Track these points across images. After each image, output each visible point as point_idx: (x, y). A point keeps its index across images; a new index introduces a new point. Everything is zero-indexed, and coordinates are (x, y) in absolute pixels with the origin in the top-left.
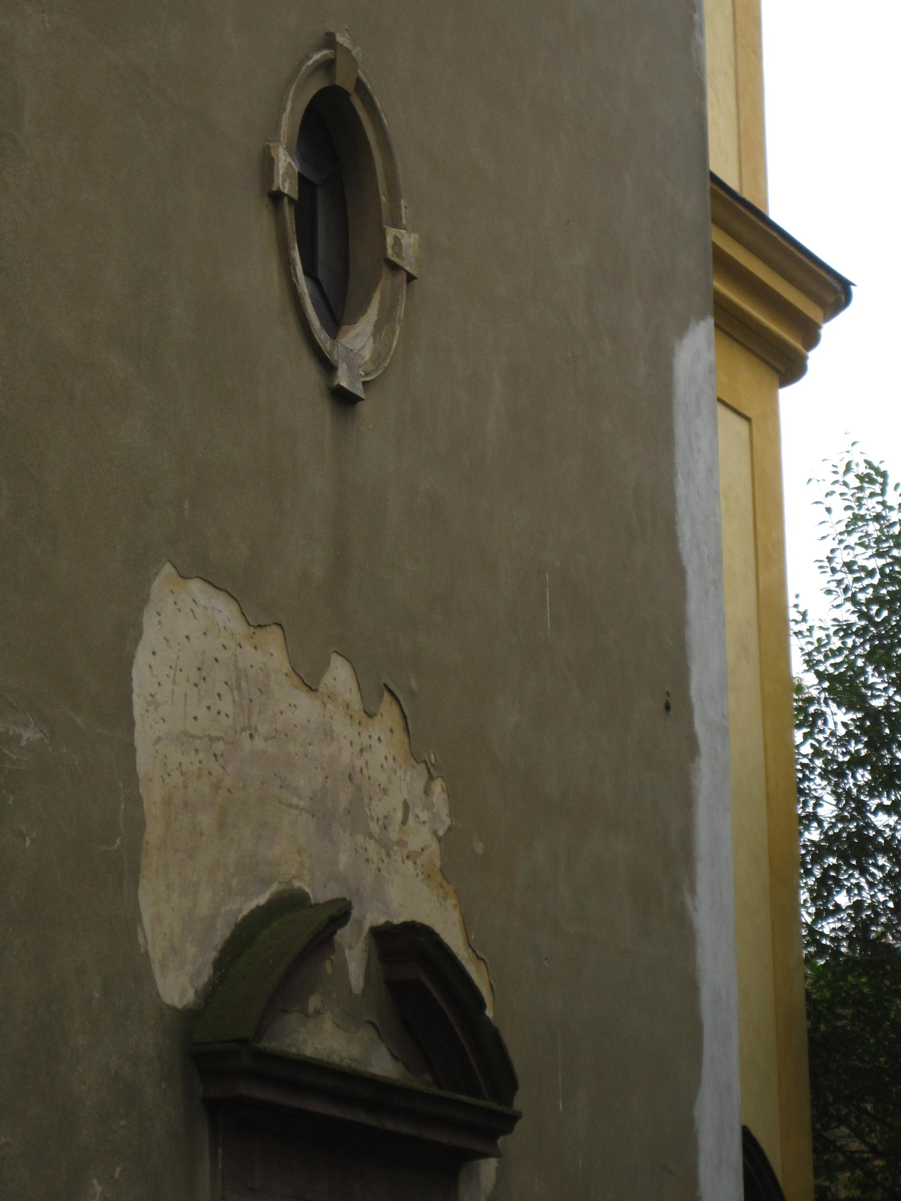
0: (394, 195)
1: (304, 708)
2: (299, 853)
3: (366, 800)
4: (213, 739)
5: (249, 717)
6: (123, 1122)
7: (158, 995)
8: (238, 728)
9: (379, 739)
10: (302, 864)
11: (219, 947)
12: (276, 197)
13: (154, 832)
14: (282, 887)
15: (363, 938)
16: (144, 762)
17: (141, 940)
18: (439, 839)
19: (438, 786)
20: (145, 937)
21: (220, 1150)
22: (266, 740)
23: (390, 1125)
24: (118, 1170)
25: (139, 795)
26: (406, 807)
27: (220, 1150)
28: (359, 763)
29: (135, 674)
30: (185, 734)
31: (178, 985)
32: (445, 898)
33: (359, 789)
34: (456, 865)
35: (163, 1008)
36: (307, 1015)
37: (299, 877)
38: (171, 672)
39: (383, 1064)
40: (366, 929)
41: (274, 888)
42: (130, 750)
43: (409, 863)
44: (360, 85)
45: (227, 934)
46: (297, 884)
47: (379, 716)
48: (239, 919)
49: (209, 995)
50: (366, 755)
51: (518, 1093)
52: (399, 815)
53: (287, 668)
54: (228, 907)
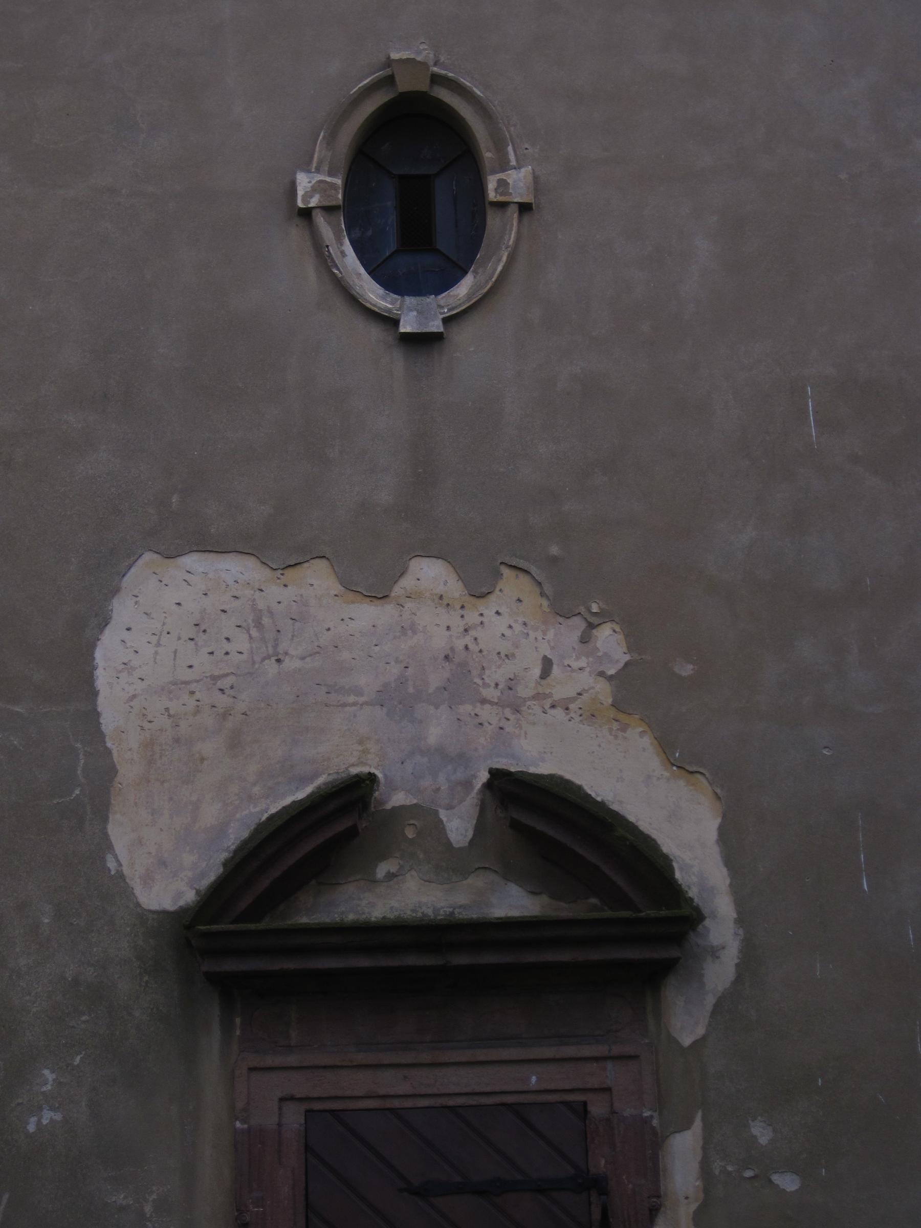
0: (499, 146)
2: (361, 742)
3: (475, 673)
4: (215, 678)
5: (276, 646)
6: (84, 1018)
7: (138, 905)
8: (257, 659)
9: (498, 613)
10: (365, 751)
11: (233, 847)
12: (306, 214)
14: (331, 778)
15: (474, 793)
17: (111, 864)
18: (610, 678)
20: (118, 861)
21: (238, 1021)
22: (303, 658)
23: (462, 960)
24: (78, 1059)
25: (106, 748)
26: (547, 666)
27: (238, 1021)
28: (460, 644)
29: (98, 654)
30: (175, 684)
32: (624, 728)
35: (142, 915)
36: (375, 881)
38: (154, 639)
39: (513, 902)
41: (321, 780)
42: (92, 716)
43: (559, 713)
44: (436, 79)
45: (245, 834)
47: (497, 592)
48: (264, 818)
50: (473, 633)
52: (537, 671)
53: (337, 588)
54: (247, 812)
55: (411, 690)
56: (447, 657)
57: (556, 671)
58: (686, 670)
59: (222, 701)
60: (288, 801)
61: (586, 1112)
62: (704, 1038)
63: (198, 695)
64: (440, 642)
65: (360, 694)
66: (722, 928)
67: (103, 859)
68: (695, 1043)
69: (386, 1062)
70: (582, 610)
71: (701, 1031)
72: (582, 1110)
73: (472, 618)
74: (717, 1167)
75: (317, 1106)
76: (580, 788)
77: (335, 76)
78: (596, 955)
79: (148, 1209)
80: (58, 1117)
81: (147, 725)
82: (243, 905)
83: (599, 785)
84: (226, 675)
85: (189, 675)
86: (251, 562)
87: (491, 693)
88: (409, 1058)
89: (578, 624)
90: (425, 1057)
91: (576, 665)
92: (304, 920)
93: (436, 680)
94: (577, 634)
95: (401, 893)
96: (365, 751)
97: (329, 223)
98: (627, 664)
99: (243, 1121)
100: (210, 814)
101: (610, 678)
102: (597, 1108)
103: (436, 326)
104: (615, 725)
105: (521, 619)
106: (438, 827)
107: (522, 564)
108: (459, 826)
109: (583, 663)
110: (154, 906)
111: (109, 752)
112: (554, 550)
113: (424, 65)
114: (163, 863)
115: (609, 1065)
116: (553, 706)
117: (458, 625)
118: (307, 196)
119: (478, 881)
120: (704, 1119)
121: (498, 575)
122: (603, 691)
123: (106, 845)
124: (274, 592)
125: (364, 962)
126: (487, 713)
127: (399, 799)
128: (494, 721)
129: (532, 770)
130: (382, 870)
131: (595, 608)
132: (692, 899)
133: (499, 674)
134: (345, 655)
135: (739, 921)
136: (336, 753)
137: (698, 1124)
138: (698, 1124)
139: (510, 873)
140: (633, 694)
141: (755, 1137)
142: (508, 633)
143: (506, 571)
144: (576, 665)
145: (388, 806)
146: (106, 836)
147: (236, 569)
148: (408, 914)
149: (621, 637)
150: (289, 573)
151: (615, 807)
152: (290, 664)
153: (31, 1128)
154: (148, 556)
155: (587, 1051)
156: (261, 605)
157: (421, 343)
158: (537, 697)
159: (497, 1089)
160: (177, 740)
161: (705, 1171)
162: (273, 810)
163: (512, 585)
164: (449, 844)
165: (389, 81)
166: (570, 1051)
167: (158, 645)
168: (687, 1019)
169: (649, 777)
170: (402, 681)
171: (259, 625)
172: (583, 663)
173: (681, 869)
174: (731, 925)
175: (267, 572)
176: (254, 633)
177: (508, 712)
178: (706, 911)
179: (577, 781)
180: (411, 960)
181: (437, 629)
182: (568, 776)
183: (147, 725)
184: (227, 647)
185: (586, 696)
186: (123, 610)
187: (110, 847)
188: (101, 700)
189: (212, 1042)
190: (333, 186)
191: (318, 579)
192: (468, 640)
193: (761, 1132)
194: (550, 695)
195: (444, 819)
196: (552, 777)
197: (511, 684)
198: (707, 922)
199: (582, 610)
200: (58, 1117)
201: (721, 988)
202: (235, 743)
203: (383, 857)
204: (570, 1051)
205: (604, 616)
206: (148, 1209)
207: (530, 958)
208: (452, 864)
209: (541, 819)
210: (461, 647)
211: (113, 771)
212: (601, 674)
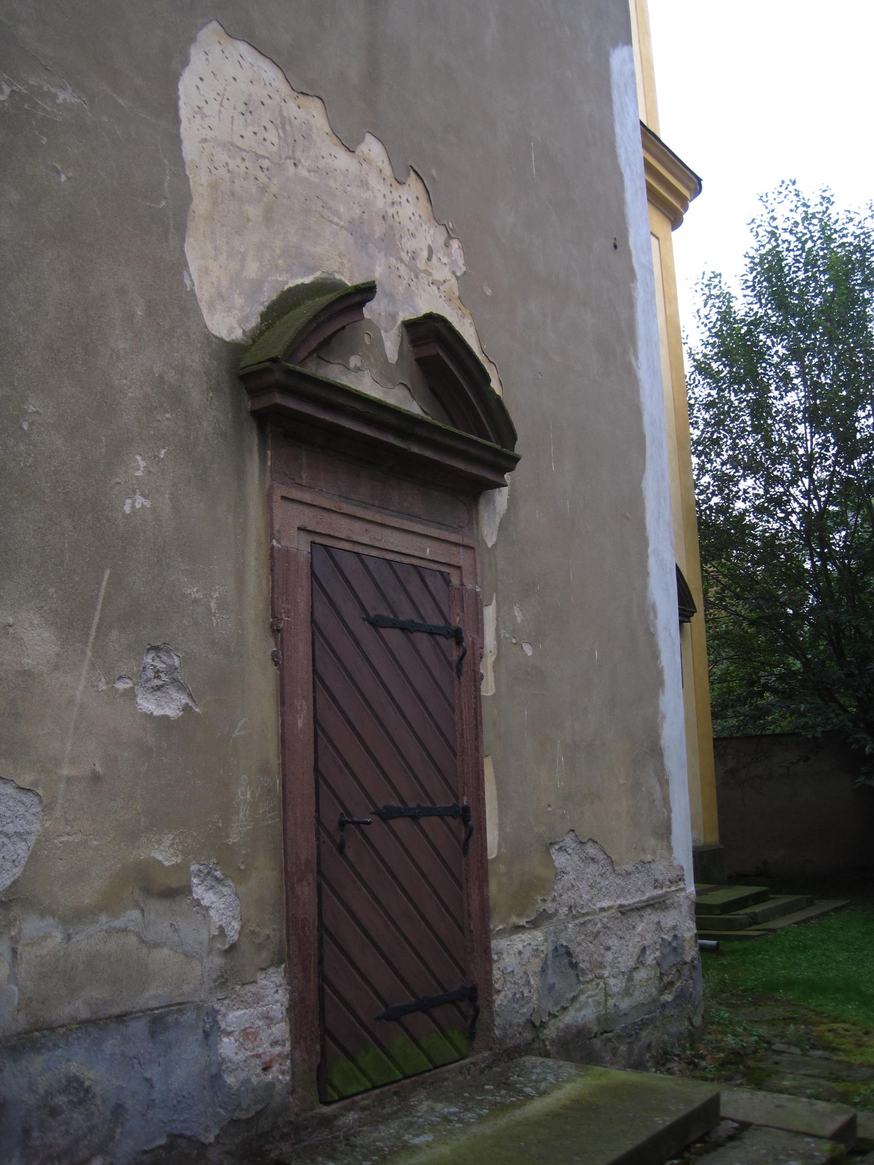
1: (343, 160)
2: (340, 255)
3: (397, 237)
4: (258, 156)
5: (294, 151)
6: (168, 415)
7: (205, 326)
8: (283, 156)
9: (407, 200)
10: (342, 264)
11: (266, 304)
13: (200, 205)
14: (324, 276)
15: (396, 327)
16: (190, 149)
17: (187, 281)
18: (457, 278)
19: (455, 244)
20: (192, 280)
21: (269, 452)
22: (309, 171)
23: (415, 449)
24: (163, 452)
25: (185, 175)
27: (269, 452)
29: (181, 86)
33: (391, 227)
34: (468, 291)
35: (209, 337)
40: (399, 322)
41: (318, 274)
42: (177, 140)
43: (434, 288)
45: (274, 297)
46: (338, 277)
48: (285, 289)
49: (256, 336)
51: (517, 443)
52: (425, 254)
53: (327, 129)
54: (274, 278)
60: (299, 281)
64: (380, 203)
65: (340, 219)
69: (358, 515)
71: (495, 539)
74: (502, 632)
75: (318, 540)
79: (213, 605)
80: (148, 504)
81: (214, 171)
84: (265, 157)
85: (239, 143)
90: (378, 518)
99: (278, 542)
100: (252, 269)
110: (216, 333)
114: (221, 296)
115: (461, 550)
120: (497, 600)
137: (494, 602)
138: (494, 602)
143: (412, 174)
153: (127, 509)
159: (411, 553)
161: (498, 637)
162: (292, 284)
175: (285, 88)
180: (391, 439)
183: (214, 171)
187: (186, 265)
189: (253, 466)
200: (148, 504)
202: (268, 216)
203: (353, 353)
206: (213, 605)
208: (386, 375)
211: (187, 197)
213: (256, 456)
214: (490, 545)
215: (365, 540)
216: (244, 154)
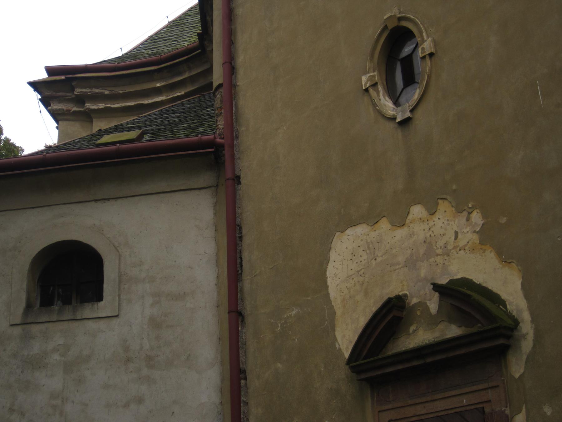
1: (400, 233)
2: (401, 282)
3: (434, 245)
4: (358, 271)
9: (439, 219)
10: (403, 285)
13: (339, 312)
17: (337, 346)
18: (478, 232)
22: (382, 256)
23: (429, 360)
26: (456, 233)
28: (428, 235)
29: (328, 273)
31: (347, 355)
37: (403, 290)
39: (454, 331)
43: (462, 251)
44: (400, 19)
47: (438, 210)
50: (432, 229)
52: (453, 238)
53: (389, 226)
55: (415, 258)
56: (424, 242)
57: (460, 236)
58: (503, 220)
59: (361, 279)
61: (484, 411)
62: (523, 374)
63: (354, 279)
64: (422, 237)
66: (527, 327)
67: (335, 345)
68: (521, 376)
69: (417, 402)
70: (466, 208)
72: (483, 410)
73: (431, 223)
76: (471, 280)
77: (371, 32)
78: (473, 349)
81: (342, 294)
82: (364, 353)
83: (478, 278)
85: (351, 273)
86: (365, 226)
87: (439, 251)
88: (424, 399)
89: (465, 213)
90: (429, 399)
91: (465, 231)
92: (390, 353)
93: (422, 251)
94: (465, 218)
95: (419, 336)
96: (403, 285)
97: (374, 90)
98: (483, 225)
101: (478, 232)
102: (487, 410)
103: (408, 114)
104: (481, 251)
105: (446, 219)
106: (427, 308)
107: (444, 196)
108: (433, 306)
109: (468, 229)
111: (333, 306)
112: (454, 187)
113: (395, 16)
115: (489, 391)
116: (460, 250)
117: (427, 227)
118: (366, 83)
119: (441, 326)
120: (526, 408)
121: (437, 204)
122: (476, 238)
123: (335, 340)
124: (373, 234)
125: (400, 367)
126: (439, 259)
127: (414, 301)
128: (441, 262)
129: (455, 278)
130: (411, 330)
131: (470, 206)
132: (514, 316)
133: (441, 243)
134: (394, 251)
135: (532, 321)
136: (394, 289)
137: (524, 410)
138: (524, 410)
139: (451, 320)
140: (487, 237)
141: (545, 413)
142: (443, 225)
143: (440, 201)
144: (465, 231)
145: (411, 305)
146: (335, 336)
147: (361, 230)
148: (421, 344)
149: (480, 214)
150: (376, 226)
151: (484, 285)
152: (379, 259)
154: (338, 234)
155: (481, 387)
156: (369, 241)
157: (405, 122)
158: (455, 248)
159: (453, 407)
160: (350, 297)
163: (443, 206)
164: (431, 313)
165: (386, 27)
166: (475, 388)
167: (343, 265)
168: (517, 367)
169: (495, 269)
170: (412, 255)
171: (369, 248)
172: (468, 229)
173: (509, 304)
174: (530, 323)
176: (368, 251)
177: (445, 257)
178: (520, 320)
179: (470, 278)
180: (415, 363)
181: (420, 231)
182: (468, 277)
183: (342, 294)
184: (362, 259)
185: (470, 243)
186: (333, 255)
187: (336, 340)
188: (329, 288)
190: (374, 76)
191: (384, 224)
192: (430, 233)
193: (548, 410)
194: (458, 246)
195: (429, 305)
196: (462, 278)
197: (446, 244)
198: (521, 324)
199: (466, 208)
201: (528, 352)
202: (366, 294)
203: (411, 325)
204: (475, 388)
205: (474, 208)
207: (451, 354)
208: (433, 322)
209: (460, 297)
210: (429, 236)
211: (335, 313)
212: (475, 232)
213: (370, 399)
214: (517, 376)
215: (424, 411)
216: (353, 276)
